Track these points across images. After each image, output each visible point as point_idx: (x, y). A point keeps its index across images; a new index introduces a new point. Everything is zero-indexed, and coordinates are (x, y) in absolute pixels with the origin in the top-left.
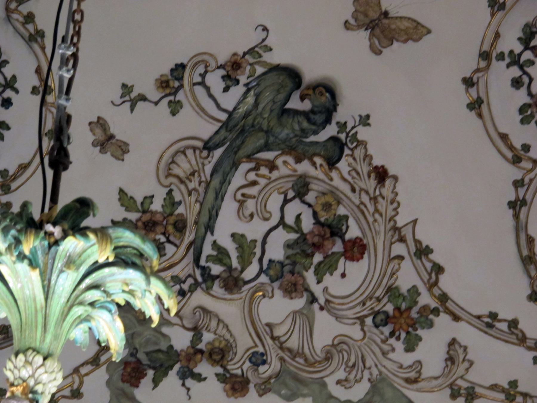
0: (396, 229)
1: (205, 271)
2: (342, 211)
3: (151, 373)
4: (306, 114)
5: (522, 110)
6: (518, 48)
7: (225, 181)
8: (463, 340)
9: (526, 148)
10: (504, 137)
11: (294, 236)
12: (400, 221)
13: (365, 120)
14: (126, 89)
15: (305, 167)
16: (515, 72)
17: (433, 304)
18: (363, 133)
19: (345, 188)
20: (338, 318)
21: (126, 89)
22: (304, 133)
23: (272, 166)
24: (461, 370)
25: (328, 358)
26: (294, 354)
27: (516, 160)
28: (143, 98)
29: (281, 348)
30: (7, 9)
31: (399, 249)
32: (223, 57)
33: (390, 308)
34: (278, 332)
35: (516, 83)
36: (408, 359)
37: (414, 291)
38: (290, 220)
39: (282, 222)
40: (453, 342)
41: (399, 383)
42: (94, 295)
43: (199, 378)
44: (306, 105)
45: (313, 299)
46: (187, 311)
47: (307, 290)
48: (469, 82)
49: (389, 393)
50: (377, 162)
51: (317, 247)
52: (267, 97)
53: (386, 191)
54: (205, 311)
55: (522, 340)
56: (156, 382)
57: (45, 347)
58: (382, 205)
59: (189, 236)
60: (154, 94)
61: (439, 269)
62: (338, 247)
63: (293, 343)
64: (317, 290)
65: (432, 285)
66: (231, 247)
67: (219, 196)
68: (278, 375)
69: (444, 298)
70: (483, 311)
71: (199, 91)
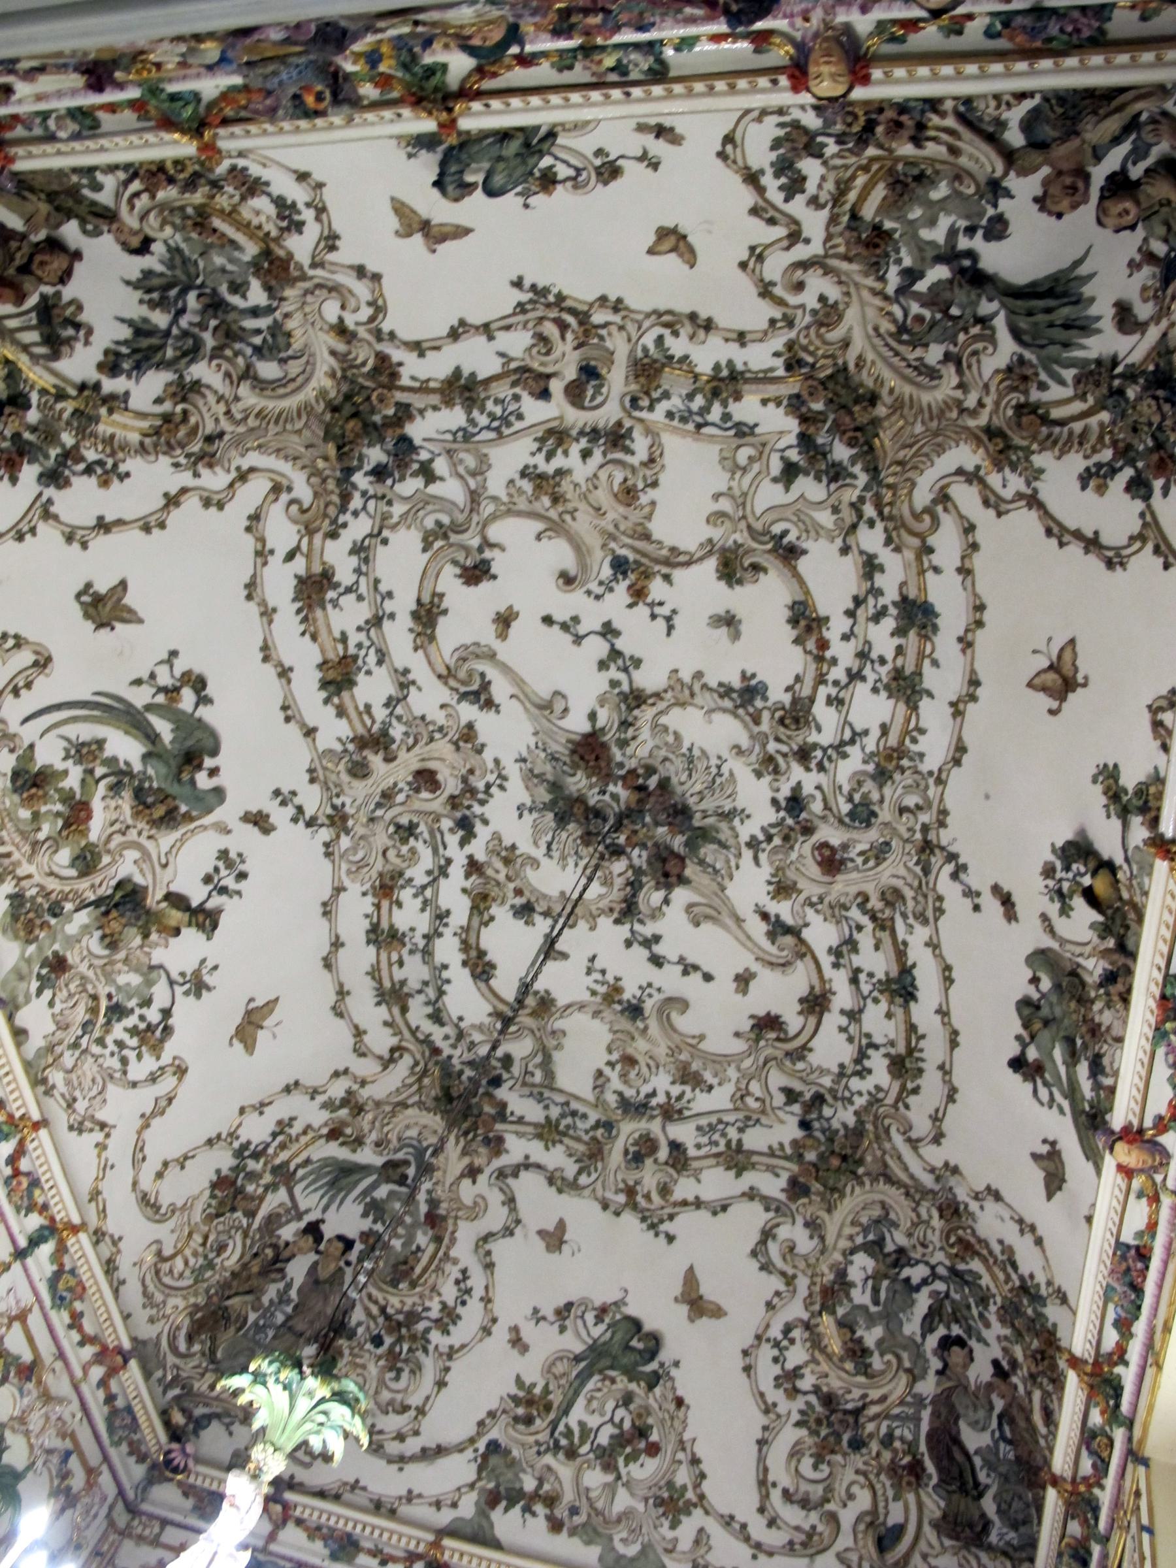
0: (681, 1442)
1: (556, 1442)
2: (650, 1421)
3: (504, 1503)
4: (640, 1352)
5: (777, 1378)
6: (780, 1337)
7: (583, 1384)
8: (709, 1530)
9: (775, 1405)
10: (762, 1395)
11: (616, 1431)
12: (687, 1436)
13: (676, 1364)
14: (536, 1311)
15: (633, 1386)
16: (776, 1352)
17: (694, 1499)
18: (674, 1372)
19: (655, 1406)
20: (632, 1494)
21: (536, 1311)
22: (637, 1364)
23: (613, 1381)
24: (702, 1551)
25: (619, 1521)
26: (598, 1513)
27: (767, 1411)
28: (544, 1318)
29: (591, 1506)
30: (477, 1246)
31: (680, 1456)
32: (598, 1304)
33: (666, 1495)
34: (593, 1495)
35: (776, 1360)
36: (670, 1535)
37: (684, 1488)
38: (617, 1419)
39: (612, 1420)
40: (701, 1530)
41: (660, 1551)
42: (321, 1418)
43: (534, 1514)
44: (640, 1346)
45: (619, 1477)
46: (538, 1466)
47: (616, 1469)
48: (745, 1353)
49: (651, 1556)
50: (679, 1393)
51: (629, 1442)
52: (618, 1336)
53: (681, 1414)
54: (549, 1468)
55: (747, 1539)
56: (506, 1510)
57: (279, 1443)
58: (676, 1423)
59: (552, 1416)
60: (552, 1317)
61: (703, 1476)
62: (642, 1445)
63: (599, 1505)
64: (623, 1471)
65: (697, 1486)
66: (576, 1430)
67: (577, 1394)
68: (584, 1525)
69: (702, 1497)
70: (725, 1511)
71: (579, 1322)
